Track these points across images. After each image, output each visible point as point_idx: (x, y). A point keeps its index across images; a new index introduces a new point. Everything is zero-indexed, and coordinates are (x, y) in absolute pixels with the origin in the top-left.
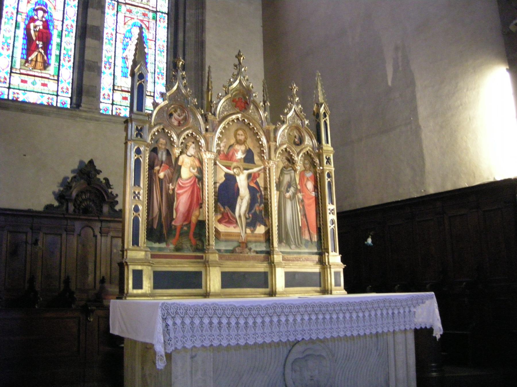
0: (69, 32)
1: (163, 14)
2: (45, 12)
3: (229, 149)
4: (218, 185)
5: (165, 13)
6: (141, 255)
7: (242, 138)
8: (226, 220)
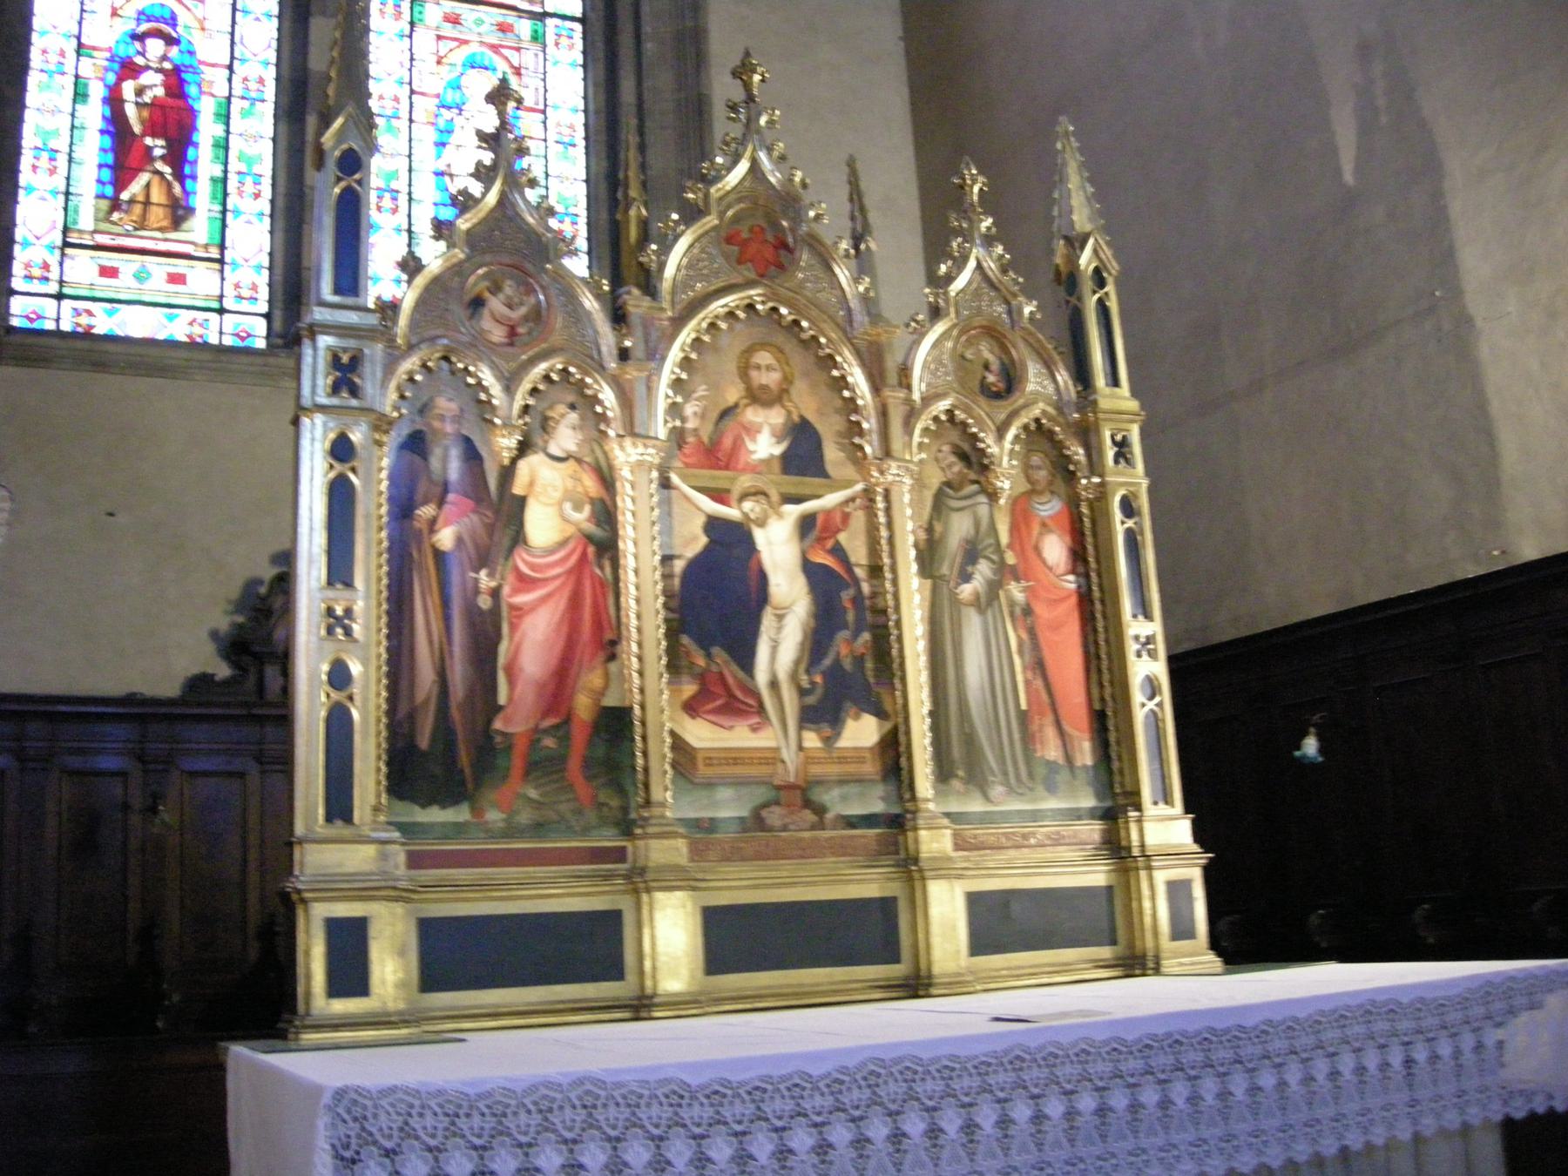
1: (569, 24)
2: (171, 41)
3: (721, 425)
4: (679, 566)
5: (573, 19)
6: (358, 858)
7: (771, 379)
8: (719, 702)
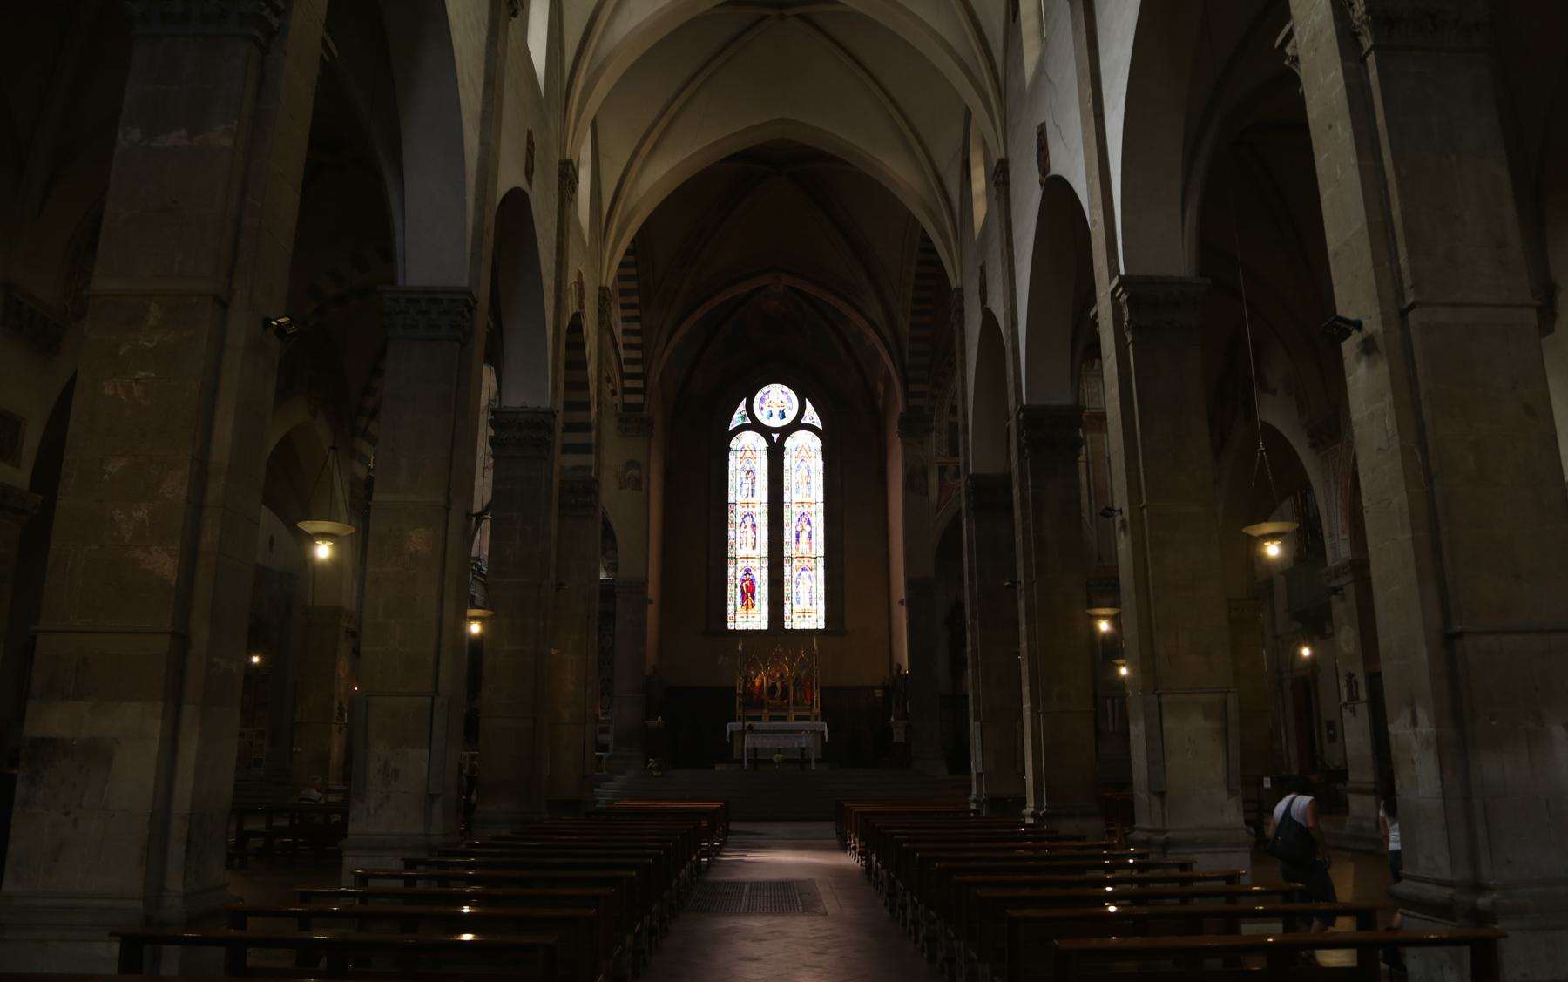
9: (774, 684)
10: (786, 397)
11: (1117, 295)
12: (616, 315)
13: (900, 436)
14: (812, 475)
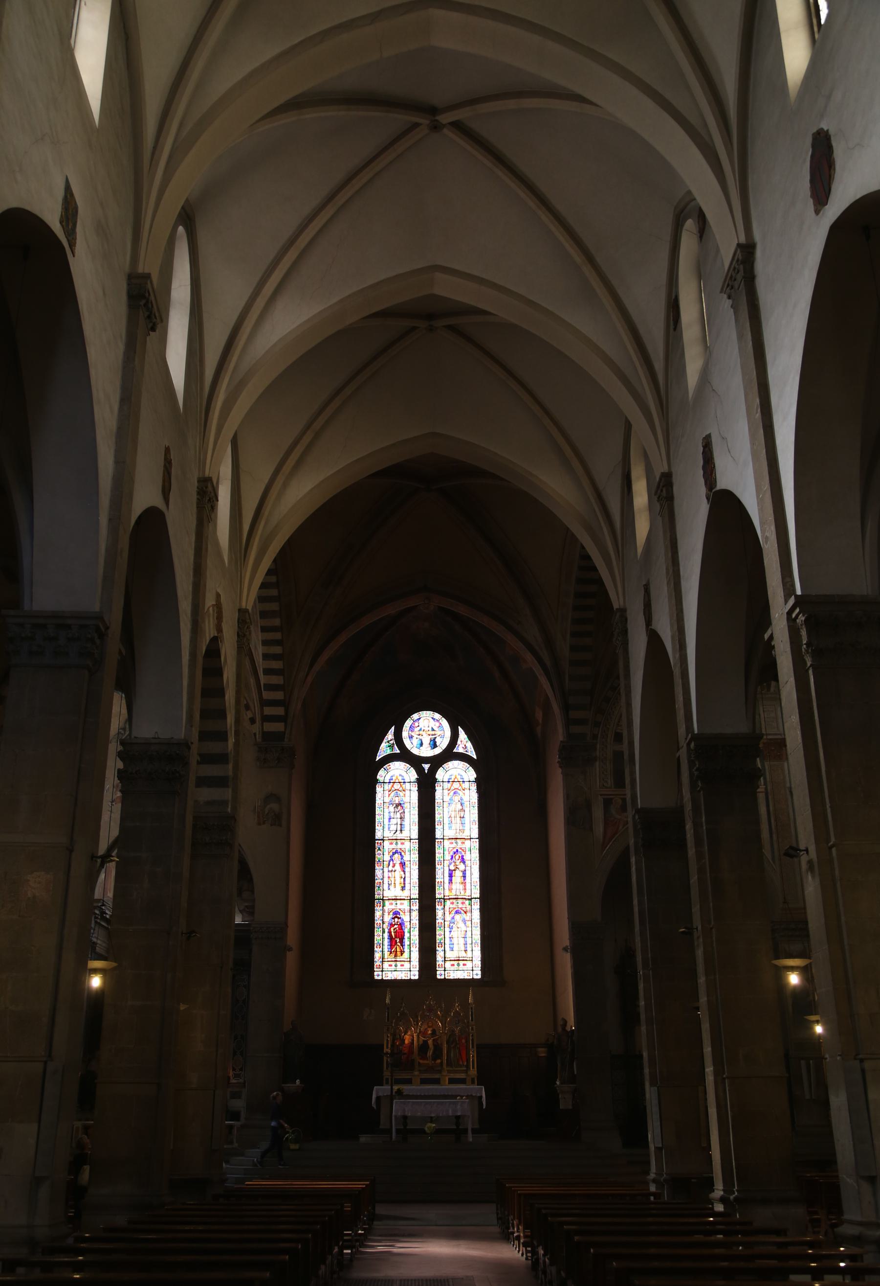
0: (414, 928)
1: (476, 900)
7: (430, 1025)
9: (425, 1042)
10: (438, 724)
11: (794, 616)
12: (256, 639)
13: (561, 767)
14: (467, 810)
